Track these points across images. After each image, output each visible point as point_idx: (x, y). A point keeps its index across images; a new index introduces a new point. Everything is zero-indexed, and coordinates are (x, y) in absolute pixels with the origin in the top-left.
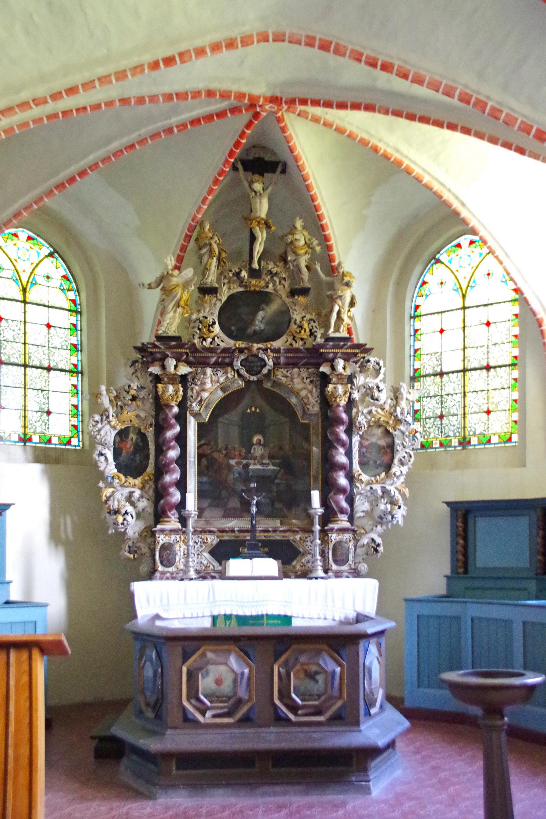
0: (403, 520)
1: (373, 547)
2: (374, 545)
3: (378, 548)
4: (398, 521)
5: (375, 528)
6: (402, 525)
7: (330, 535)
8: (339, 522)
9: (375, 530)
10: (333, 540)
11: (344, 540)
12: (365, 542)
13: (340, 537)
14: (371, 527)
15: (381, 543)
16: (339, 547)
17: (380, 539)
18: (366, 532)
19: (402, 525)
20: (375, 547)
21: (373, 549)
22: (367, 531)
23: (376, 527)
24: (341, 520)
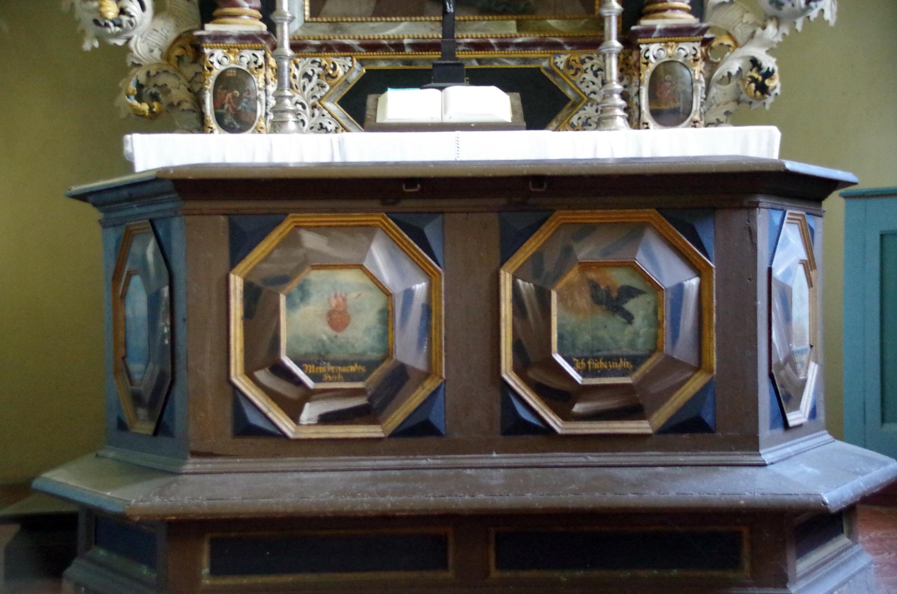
0: (835, 8)
1: (754, 80)
2: (756, 75)
3: (767, 82)
4: (822, 10)
5: (759, 31)
6: (832, 22)
7: (643, 47)
8: (669, 13)
9: (761, 37)
10: (652, 58)
11: (681, 60)
12: (734, 70)
13: (670, 51)
14: (750, 30)
15: (776, 69)
16: (668, 77)
17: (774, 60)
18: (737, 45)
19: (832, 22)
20: (760, 78)
21: (753, 85)
22: (740, 41)
23: (764, 28)
24: (674, 9)
